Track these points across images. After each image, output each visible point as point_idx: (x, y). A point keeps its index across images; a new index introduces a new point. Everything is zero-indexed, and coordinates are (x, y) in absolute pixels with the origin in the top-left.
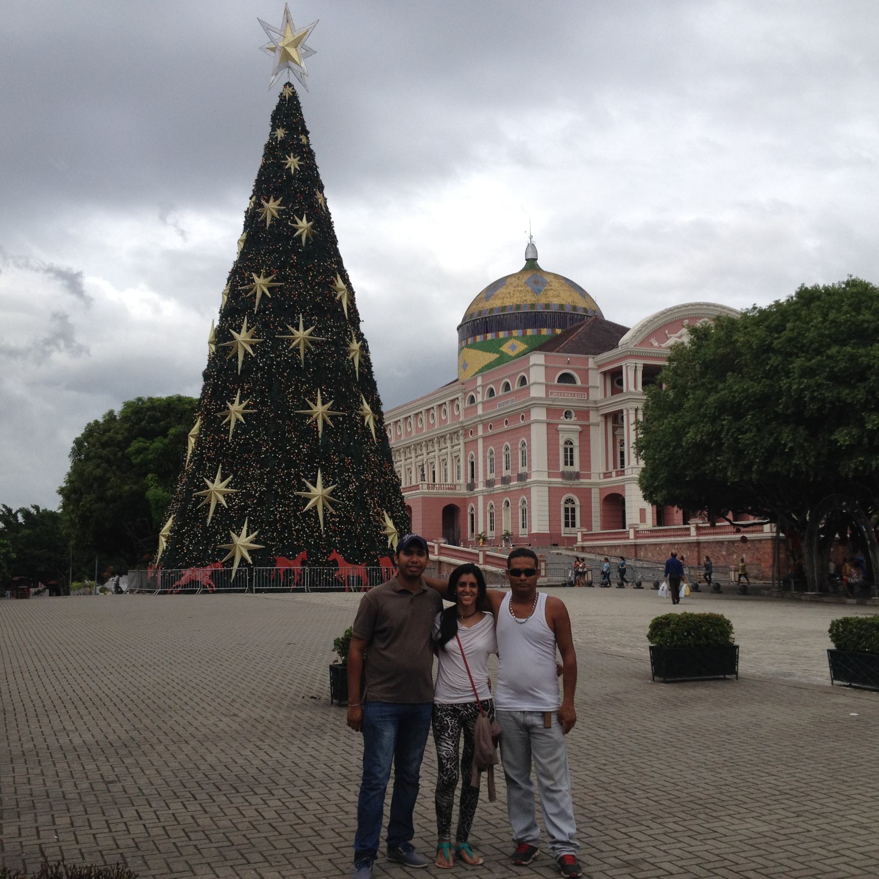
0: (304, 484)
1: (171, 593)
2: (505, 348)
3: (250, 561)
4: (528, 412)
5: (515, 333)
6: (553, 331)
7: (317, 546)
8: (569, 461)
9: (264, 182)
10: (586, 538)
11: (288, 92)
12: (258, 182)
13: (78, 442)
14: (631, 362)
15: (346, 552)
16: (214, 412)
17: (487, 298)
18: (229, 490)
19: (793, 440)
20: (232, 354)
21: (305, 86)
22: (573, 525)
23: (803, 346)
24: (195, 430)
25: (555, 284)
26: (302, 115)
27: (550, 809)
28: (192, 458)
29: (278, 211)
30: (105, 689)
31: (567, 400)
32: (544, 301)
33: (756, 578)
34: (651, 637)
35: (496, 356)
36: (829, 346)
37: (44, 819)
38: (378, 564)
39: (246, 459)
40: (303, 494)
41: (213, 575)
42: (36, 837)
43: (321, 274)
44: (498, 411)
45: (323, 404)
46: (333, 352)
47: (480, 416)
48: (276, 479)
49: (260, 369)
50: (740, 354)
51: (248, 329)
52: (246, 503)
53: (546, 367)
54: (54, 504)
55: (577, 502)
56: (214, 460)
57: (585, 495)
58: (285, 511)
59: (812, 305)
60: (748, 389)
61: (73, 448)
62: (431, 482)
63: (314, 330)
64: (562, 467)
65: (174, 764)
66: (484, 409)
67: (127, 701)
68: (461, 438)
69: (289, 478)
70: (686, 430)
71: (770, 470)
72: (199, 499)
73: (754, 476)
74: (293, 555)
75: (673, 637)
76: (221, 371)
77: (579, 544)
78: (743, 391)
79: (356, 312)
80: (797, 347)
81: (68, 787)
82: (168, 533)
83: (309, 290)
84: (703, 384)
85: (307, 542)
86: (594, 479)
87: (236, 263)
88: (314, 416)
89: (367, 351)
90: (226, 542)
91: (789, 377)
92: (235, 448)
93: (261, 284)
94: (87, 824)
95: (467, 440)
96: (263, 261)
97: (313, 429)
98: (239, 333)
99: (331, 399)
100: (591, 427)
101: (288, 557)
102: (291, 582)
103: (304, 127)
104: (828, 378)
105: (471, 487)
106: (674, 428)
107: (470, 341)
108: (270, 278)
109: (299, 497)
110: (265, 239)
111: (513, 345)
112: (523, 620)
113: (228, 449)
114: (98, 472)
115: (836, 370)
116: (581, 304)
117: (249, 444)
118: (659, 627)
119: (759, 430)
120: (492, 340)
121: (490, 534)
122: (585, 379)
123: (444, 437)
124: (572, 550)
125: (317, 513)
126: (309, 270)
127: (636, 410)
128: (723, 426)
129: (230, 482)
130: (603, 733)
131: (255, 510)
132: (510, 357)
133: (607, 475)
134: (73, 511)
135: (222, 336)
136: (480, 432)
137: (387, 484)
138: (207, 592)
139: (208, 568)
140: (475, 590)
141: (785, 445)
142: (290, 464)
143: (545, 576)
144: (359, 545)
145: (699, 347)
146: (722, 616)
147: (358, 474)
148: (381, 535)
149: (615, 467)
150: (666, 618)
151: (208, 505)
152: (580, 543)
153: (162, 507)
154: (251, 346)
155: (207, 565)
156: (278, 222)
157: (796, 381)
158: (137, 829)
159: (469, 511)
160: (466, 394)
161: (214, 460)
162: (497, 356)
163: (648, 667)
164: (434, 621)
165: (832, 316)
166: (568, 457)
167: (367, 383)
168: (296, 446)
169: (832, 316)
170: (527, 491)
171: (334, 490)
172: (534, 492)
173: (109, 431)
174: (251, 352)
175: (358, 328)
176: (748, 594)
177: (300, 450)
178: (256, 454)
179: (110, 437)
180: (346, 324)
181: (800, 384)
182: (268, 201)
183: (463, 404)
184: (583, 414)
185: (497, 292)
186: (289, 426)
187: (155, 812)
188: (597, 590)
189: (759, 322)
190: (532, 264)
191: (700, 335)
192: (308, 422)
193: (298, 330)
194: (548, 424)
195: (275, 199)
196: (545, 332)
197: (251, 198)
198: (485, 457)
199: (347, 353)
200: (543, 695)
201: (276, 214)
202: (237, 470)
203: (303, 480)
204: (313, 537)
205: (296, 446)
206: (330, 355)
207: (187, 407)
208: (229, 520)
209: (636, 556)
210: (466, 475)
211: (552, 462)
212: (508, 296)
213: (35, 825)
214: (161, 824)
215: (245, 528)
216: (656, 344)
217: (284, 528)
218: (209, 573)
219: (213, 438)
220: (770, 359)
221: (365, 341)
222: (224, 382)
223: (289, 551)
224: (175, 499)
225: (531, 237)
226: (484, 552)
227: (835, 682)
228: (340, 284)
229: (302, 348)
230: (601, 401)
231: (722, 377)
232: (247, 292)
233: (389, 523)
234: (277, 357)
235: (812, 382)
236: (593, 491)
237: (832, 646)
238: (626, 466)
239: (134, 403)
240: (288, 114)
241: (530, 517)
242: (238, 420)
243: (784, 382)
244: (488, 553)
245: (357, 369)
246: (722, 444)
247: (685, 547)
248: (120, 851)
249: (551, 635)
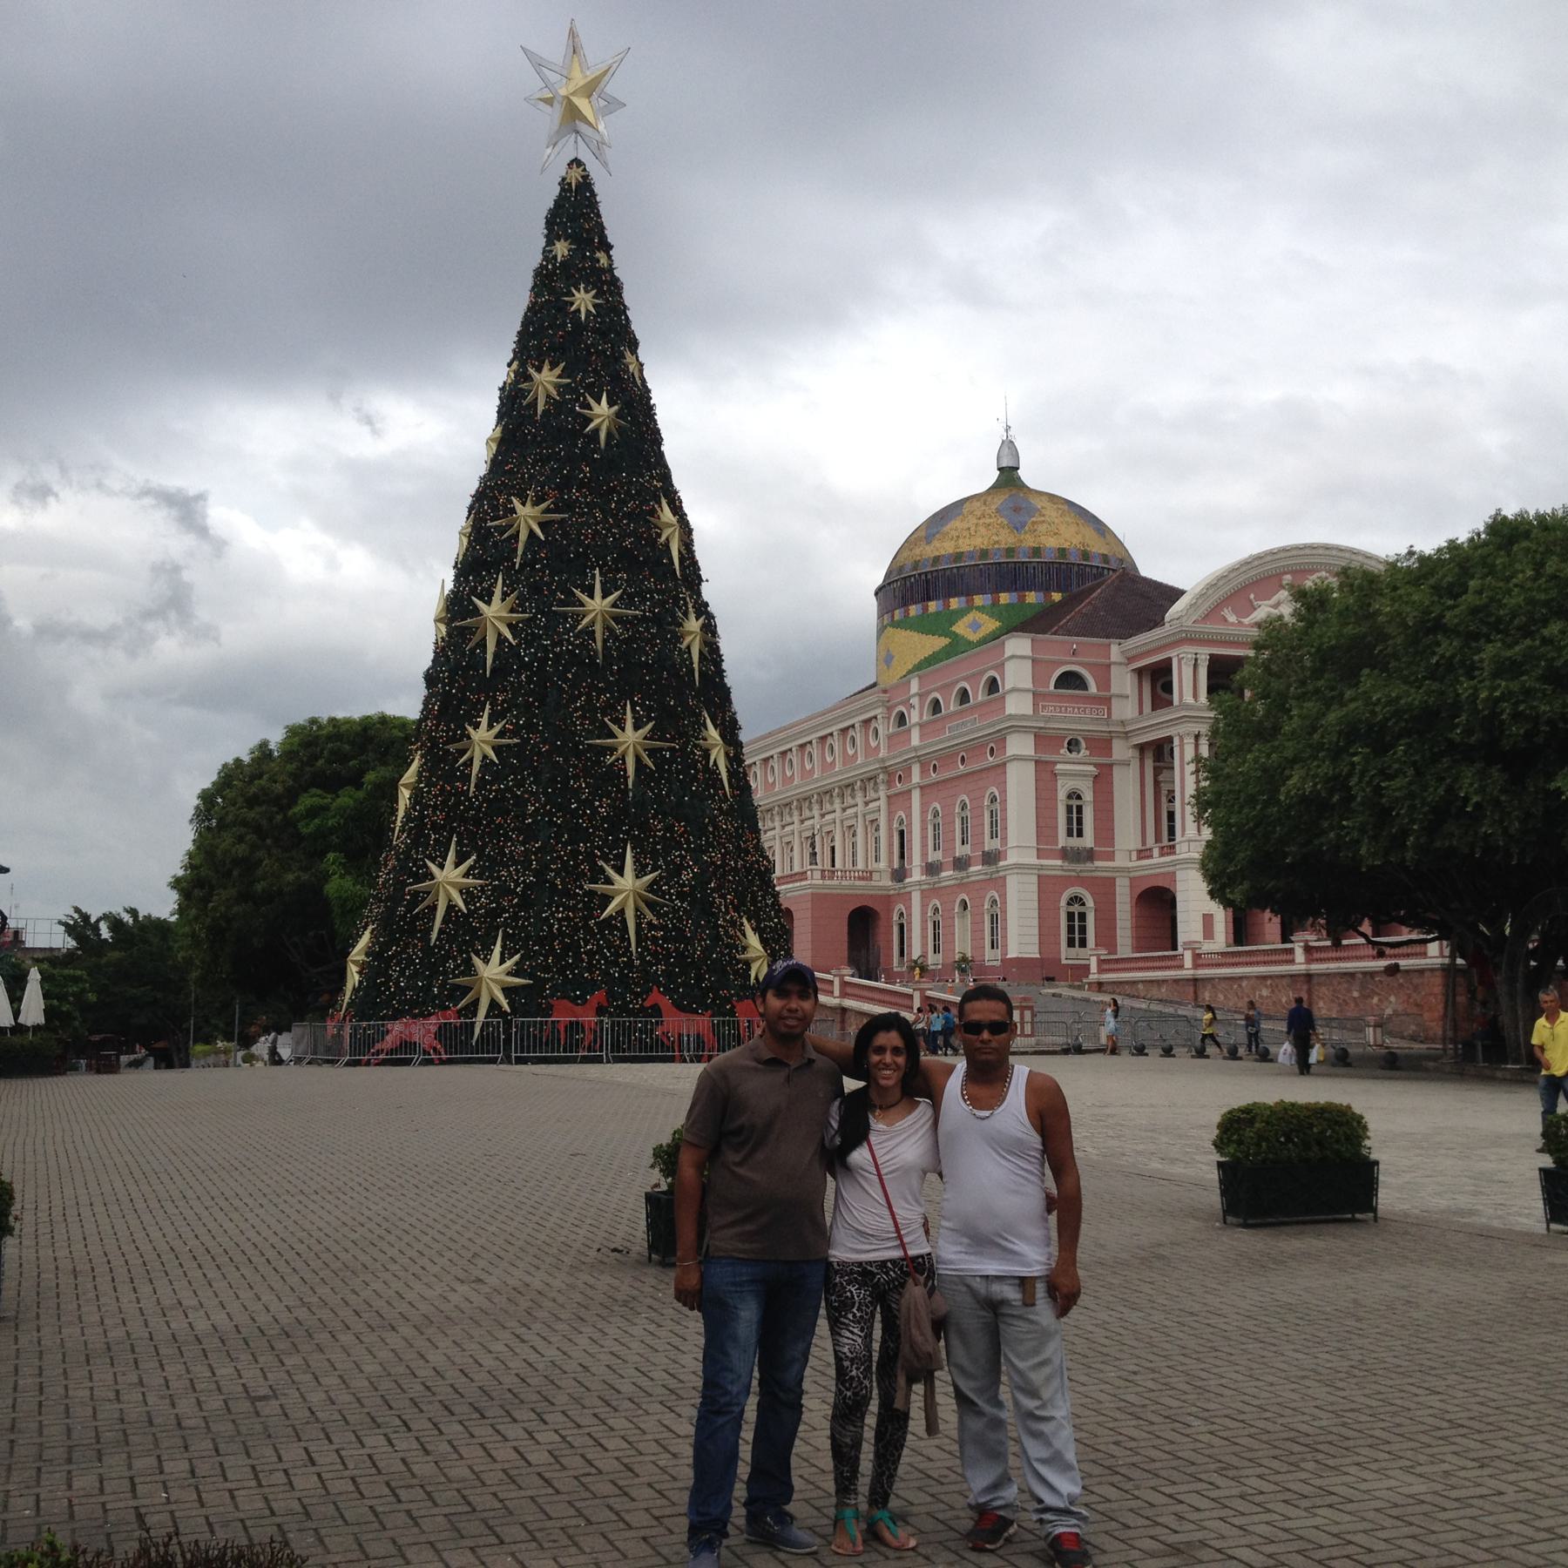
0: (603, 871)
1: (368, 1063)
2: (961, 628)
3: (506, 1008)
4: (1002, 741)
5: (979, 600)
6: (1048, 597)
7: (624, 980)
9: (533, 336)
10: (1106, 966)
11: (575, 176)
12: (523, 336)
13: (207, 797)
14: (1187, 651)
15: (675, 990)
16: (445, 743)
17: (928, 539)
18: (470, 881)
19: (1482, 790)
20: (476, 639)
21: (605, 164)
22: (1083, 944)
23: (1499, 620)
24: (410, 775)
25: (1051, 513)
26: (599, 216)
27: (1035, 1450)
28: (404, 824)
29: (557, 386)
30: (251, 1234)
31: (1073, 720)
32: (1029, 542)
33: (1413, 1038)
34: (1219, 1145)
35: (942, 642)
36: (1545, 622)
37: (143, 1463)
38: (732, 1013)
39: (500, 826)
40: (600, 887)
41: (443, 1032)
42: (129, 1495)
43: (632, 497)
44: (949, 739)
45: (636, 728)
46: (654, 636)
47: (915, 749)
48: (553, 861)
49: (524, 666)
50: (1383, 637)
51: (505, 595)
52: (499, 904)
53: (1034, 661)
54: (163, 905)
55: (1090, 903)
56: (443, 827)
57: (1103, 889)
58: (567, 918)
59: (1515, 548)
60: (1398, 698)
61: (197, 808)
62: (828, 866)
63: (621, 598)
64: (1062, 840)
65: (370, 1368)
66: (922, 737)
67: (290, 1255)
68: (882, 787)
69: (575, 859)
70: (1287, 772)
71: (1438, 844)
72: (417, 897)
73: (1409, 855)
74: (582, 997)
75: (1258, 1145)
76: (457, 672)
77: (1094, 976)
78: (1389, 703)
79: (695, 563)
80: (1486, 623)
81: (186, 1406)
82: (362, 957)
83: (612, 526)
84: (1317, 691)
85: (606, 973)
86: (1120, 861)
87: (483, 480)
88: (621, 750)
89: (715, 634)
90: (463, 974)
91: (1473, 678)
92: (480, 806)
93: (527, 515)
94: (218, 1471)
95: (892, 791)
96: (532, 476)
97: (617, 772)
98: (488, 603)
99: (650, 719)
100: (1116, 770)
101: (574, 1000)
102: (577, 1046)
103: (603, 238)
104: (1544, 679)
105: (900, 875)
106: (1265, 770)
107: (898, 614)
108: (544, 506)
109: (592, 893)
110: (535, 436)
111: (975, 623)
112: (986, 1113)
113: (467, 810)
114: (241, 850)
115: (1559, 663)
116: (1097, 547)
117: (504, 799)
118: (1235, 1127)
119: (1419, 773)
120: (938, 613)
121: (933, 960)
122: (1104, 683)
123: (851, 785)
124: (1080, 988)
125: (624, 921)
126: (612, 490)
127: (1197, 737)
128: (1353, 764)
129: (472, 868)
130: (1134, 1316)
131: (515, 917)
132: (970, 643)
133: (1144, 854)
134: (196, 919)
135: (458, 608)
136: (916, 777)
137: (748, 871)
138: (429, 1062)
139: (433, 1020)
140: (901, 1060)
141: (1466, 799)
142: (578, 834)
143: (1032, 1035)
144: (699, 979)
145: (1311, 624)
146: (1349, 1107)
147: (697, 852)
148: (739, 962)
149: (1158, 839)
150: (1247, 1110)
151: (434, 908)
152: (1094, 976)
153: (353, 911)
154: (510, 626)
155: (430, 1014)
156: (556, 407)
157: (1487, 683)
158: (306, 1482)
159: (895, 918)
160: (890, 709)
161: (443, 827)
162: (947, 641)
163: (1214, 1199)
164: (827, 1113)
165: (1551, 566)
166: (1073, 821)
167: (712, 690)
168: (589, 803)
169: (1551, 566)
170: (999, 883)
171: (654, 882)
172: (1013, 883)
173: (260, 777)
174: (510, 637)
175: (699, 594)
176: (1398, 1069)
177: (595, 810)
178: (516, 817)
179: (263, 789)
180: (676, 587)
181: (1495, 689)
182: (539, 370)
183: (885, 728)
184: (1101, 745)
185: (946, 529)
186: (575, 767)
187: (337, 1451)
188: (1125, 1060)
189: (1418, 578)
190: (1009, 476)
191: (1312, 603)
192: (610, 760)
193: (592, 597)
195: (553, 366)
196: (1032, 597)
197: (509, 365)
198: (924, 822)
199: (678, 638)
200: (1021, 1247)
201: (554, 393)
202: (485, 845)
203: (601, 863)
204: (616, 964)
205: (589, 803)
206: (648, 641)
207: (396, 732)
208: (469, 933)
209: (1196, 999)
210: (891, 853)
211: (1044, 830)
212: (966, 533)
213: (127, 1474)
214: (347, 1473)
215: (498, 949)
216: (1232, 619)
217: (566, 948)
218: (434, 1029)
219: (442, 789)
220: (1438, 644)
221: (710, 617)
222: (462, 690)
223: (576, 989)
224: (375, 897)
225: (1008, 428)
226: (922, 991)
227: (1553, 1226)
228: (667, 515)
229: (598, 628)
230: (1133, 721)
231: (1352, 677)
232: (501, 530)
233: (753, 940)
234: (554, 644)
235: (1515, 686)
236: (1118, 882)
237: (1547, 1161)
239: (302, 728)
240: (576, 214)
241: (1005, 929)
242: (485, 757)
243: (1464, 687)
244: (929, 993)
245: (696, 666)
246: (1354, 798)
247: (1285, 982)
248: (278, 1520)
249: (1035, 1140)
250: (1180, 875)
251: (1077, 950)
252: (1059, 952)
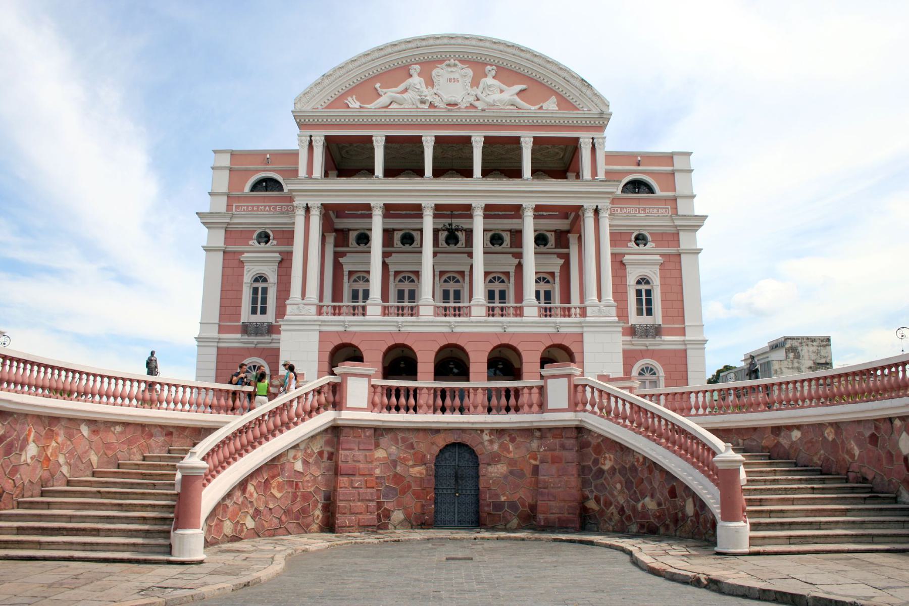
8: (258, 306)
53: (231, 170)
127: (307, 209)
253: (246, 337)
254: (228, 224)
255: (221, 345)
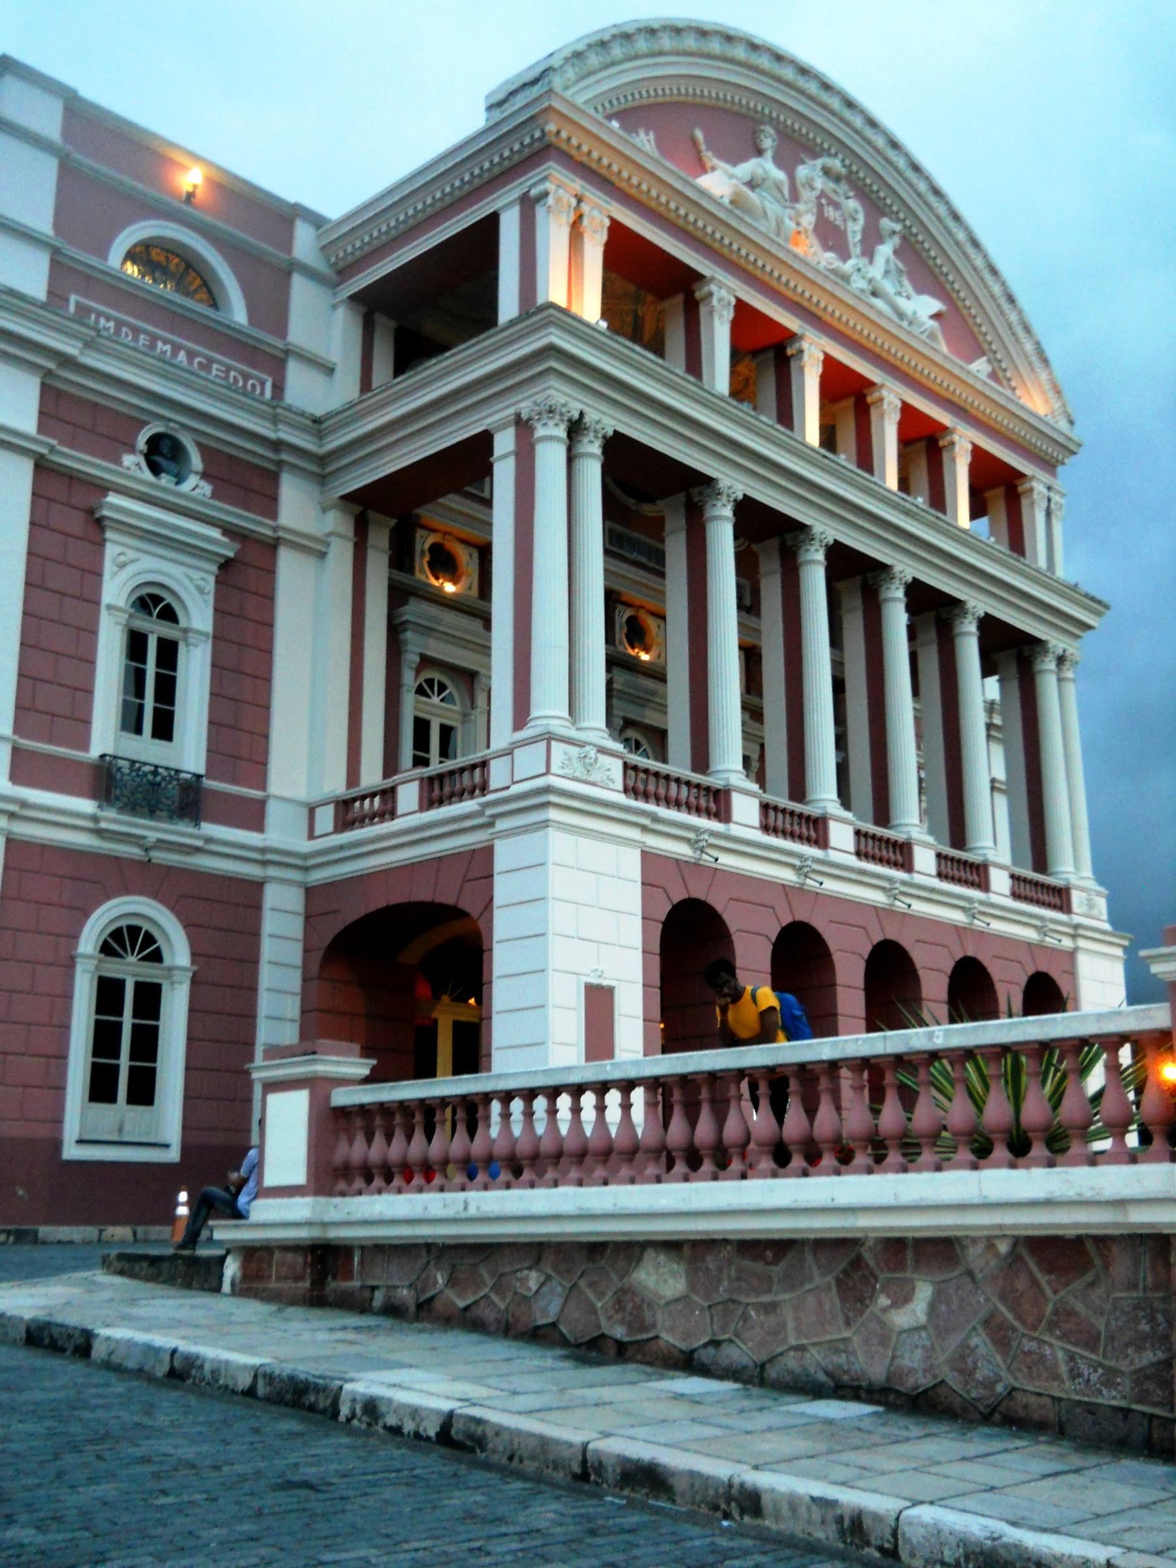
10: (357, 1150)
22: (143, 1091)
55: (178, 951)
86: (282, 831)
100: (288, 564)
127: (576, 429)
184: (247, 478)
194: (43, 468)
236: (273, 896)
238: (502, 732)
250: (505, 855)
251: (120, 1113)
252: (58, 1121)
253: (111, 813)
254: (66, 361)
255: (23, 830)
